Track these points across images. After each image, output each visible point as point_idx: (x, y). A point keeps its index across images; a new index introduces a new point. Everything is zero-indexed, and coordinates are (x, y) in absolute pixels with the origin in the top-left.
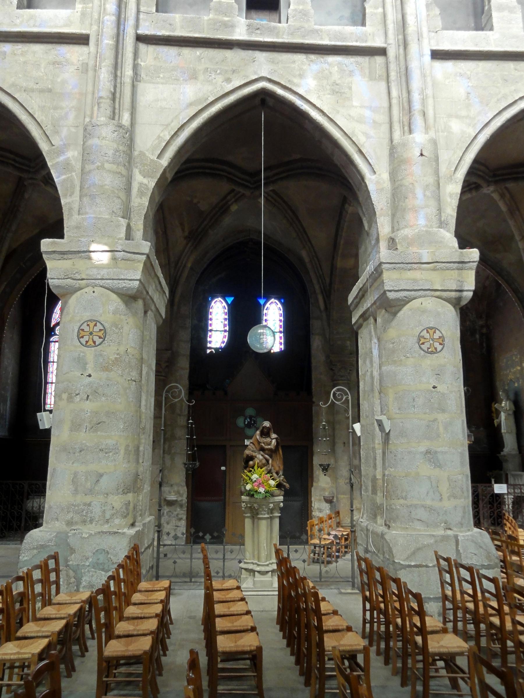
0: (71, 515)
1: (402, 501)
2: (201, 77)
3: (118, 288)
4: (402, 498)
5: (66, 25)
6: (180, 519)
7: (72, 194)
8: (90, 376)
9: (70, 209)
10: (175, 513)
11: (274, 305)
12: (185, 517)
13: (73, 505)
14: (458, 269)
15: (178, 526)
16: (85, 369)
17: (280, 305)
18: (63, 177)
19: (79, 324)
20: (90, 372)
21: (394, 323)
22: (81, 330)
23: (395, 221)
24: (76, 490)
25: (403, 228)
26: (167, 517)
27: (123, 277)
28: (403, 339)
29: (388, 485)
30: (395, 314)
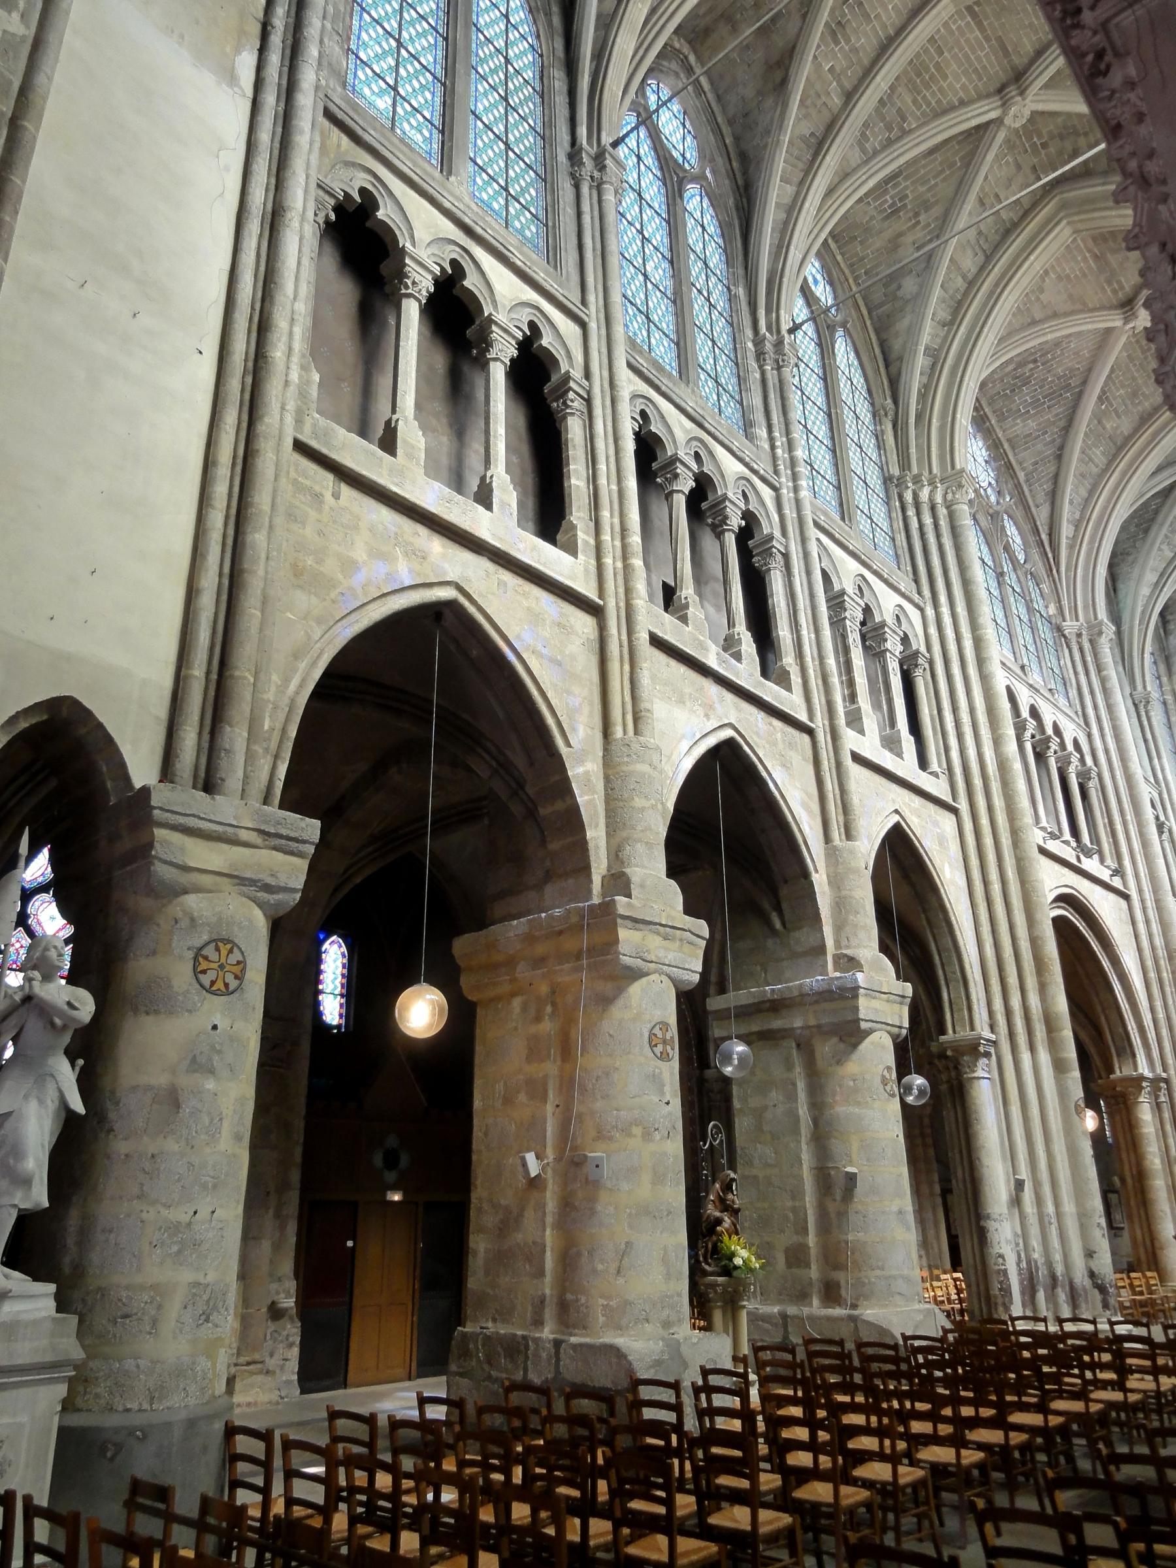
0: (666, 1312)
1: (878, 1272)
2: (688, 703)
3: (682, 981)
4: (878, 1268)
5: (570, 578)
6: (291, 1345)
7: (597, 826)
8: (668, 1103)
9: (597, 847)
10: (285, 1333)
11: (336, 946)
12: (298, 1340)
13: (667, 1296)
14: (901, 1003)
15: (286, 1360)
16: (662, 1093)
17: (344, 949)
18: (586, 798)
19: (649, 1026)
20: (668, 1097)
21: (855, 1056)
22: (652, 1035)
23: (843, 935)
24: (668, 1274)
25: (855, 947)
26: (270, 1342)
27: (687, 966)
28: (868, 1077)
29: (853, 1253)
30: (855, 1046)
